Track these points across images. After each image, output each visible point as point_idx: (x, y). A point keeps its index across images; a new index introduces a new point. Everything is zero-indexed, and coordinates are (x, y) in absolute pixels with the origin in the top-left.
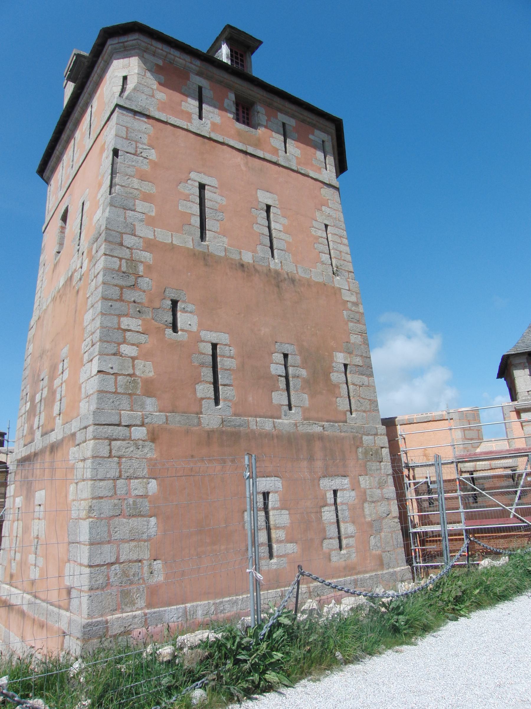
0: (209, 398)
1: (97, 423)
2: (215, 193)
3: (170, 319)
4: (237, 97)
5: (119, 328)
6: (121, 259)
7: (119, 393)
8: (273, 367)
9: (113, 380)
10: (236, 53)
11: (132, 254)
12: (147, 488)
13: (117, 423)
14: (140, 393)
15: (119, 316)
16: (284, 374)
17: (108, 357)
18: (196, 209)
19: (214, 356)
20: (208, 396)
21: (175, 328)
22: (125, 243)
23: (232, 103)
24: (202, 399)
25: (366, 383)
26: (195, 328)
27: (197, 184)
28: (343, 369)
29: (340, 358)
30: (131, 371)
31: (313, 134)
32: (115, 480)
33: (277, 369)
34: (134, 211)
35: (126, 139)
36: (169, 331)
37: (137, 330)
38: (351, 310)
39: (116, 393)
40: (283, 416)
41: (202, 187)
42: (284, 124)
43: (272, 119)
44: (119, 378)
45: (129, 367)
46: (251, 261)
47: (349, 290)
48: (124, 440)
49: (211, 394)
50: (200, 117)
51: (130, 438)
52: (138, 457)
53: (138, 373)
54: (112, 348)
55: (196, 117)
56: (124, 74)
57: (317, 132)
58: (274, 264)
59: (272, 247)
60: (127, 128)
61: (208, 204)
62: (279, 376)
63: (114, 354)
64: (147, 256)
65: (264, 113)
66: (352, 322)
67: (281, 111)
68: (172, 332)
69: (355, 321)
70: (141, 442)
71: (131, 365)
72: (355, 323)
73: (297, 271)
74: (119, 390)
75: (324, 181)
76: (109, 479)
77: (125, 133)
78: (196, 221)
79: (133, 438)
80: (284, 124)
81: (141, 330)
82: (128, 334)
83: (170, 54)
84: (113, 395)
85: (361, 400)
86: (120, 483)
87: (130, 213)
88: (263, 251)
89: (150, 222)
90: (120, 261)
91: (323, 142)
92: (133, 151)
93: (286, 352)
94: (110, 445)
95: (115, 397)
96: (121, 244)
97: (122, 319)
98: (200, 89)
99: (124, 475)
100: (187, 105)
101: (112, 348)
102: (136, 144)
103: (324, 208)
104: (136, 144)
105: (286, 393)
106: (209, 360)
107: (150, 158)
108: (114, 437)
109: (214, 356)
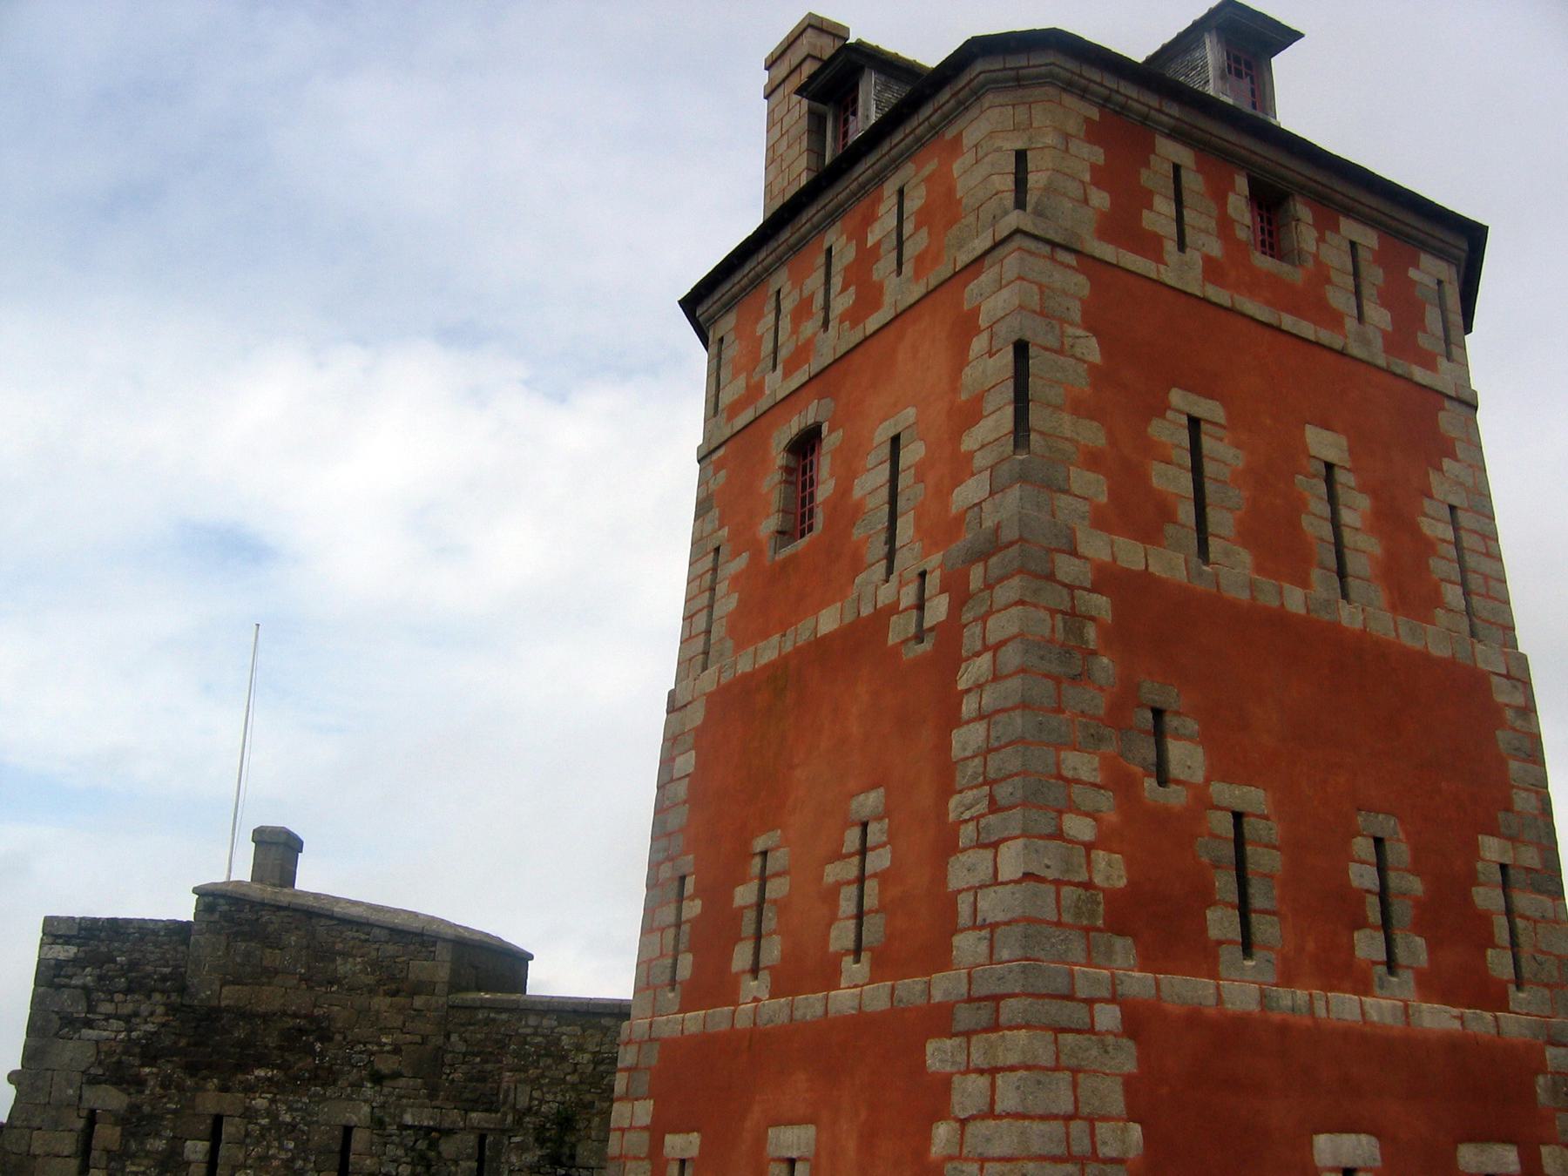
0: (1231, 942)
1: (1030, 990)
2: (1221, 440)
3: (1152, 756)
4: (1253, 183)
5: (1060, 777)
6: (1053, 612)
7: (1066, 925)
8: (1354, 869)
9: (1053, 896)
10: (1237, 60)
11: (1073, 599)
12: (1124, 1143)
13: (1066, 992)
14: (1102, 926)
15: (1058, 747)
16: (1376, 889)
17: (1041, 842)
18: (1185, 483)
19: (1239, 841)
20: (1230, 936)
21: (1163, 779)
22: (1060, 576)
23: (1244, 200)
24: (1220, 943)
25: (1550, 914)
26: (1199, 777)
27: (1185, 420)
28: (1498, 877)
29: (1492, 849)
30: (1083, 877)
31: (1417, 267)
32: (1068, 1118)
33: (1363, 876)
34: (1067, 492)
35: (1042, 313)
36: (1150, 783)
37: (1092, 780)
38: (1514, 729)
39: (1059, 924)
40: (1377, 991)
41: (1194, 423)
42: (1353, 244)
43: (1328, 234)
44: (1066, 890)
45: (1081, 867)
46: (1303, 611)
47: (1508, 676)
48: (1079, 1031)
49: (1235, 933)
50: (1182, 246)
51: (1091, 1030)
52: (1108, 1071)
53: (1098, 880)
54: (1045, 824)
55: (1171, 246)
56: (1019, 145)
57: (1426, 260)
58: (1349, 617)
59: (1342, 573)
60: (1041, 286)
61: (1209, 468)
62: (1368, 891)
63: (1050, 837)
64: (1100, 605)
65: (1311, 222)
66: (1516, 758)
67: (1349, 213)
68: (1155, 784)
69: (1523, 756)
70: (1110, 1039)
71: (1083, 861)
72: (1523, 760)
73: (1396, 630)
74: (1066, 918)
75: (1445, 391)
76: (1055, 1117)
77: (1037, 298)
78: (1186, 513)
79: (1097, 1028)
80: (1353, 244)
81: (1098, 781)
82: (1076, 789)
83: (1117, 92)
84: (1054, 929)
85: (1539, 957)
86: (1077, 1127)
87: (1063, 501)
88: (1322, 583)
89: (1100, 521)
90: (1053, 618)
91: (1440, 282)
92: (1056, 345)
93: (1379, 835)
94: (1056, 1040)
95: (1058, 933)
96: (1050, 577)
97: (1063, 754)
98: (1177, 168)
99: (1085, 1110)
100: (1152, 215)
101: (1045, 824)
102: (1061, 328)
103: (1447, 463)
104: (1061, 328)
105: (1380, 936)
106: (1229, 851)
107: (1090, 358)
108: (1064, 1024)
109: (1239, 841)
